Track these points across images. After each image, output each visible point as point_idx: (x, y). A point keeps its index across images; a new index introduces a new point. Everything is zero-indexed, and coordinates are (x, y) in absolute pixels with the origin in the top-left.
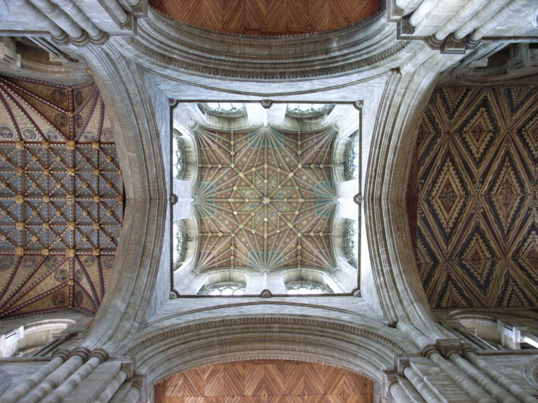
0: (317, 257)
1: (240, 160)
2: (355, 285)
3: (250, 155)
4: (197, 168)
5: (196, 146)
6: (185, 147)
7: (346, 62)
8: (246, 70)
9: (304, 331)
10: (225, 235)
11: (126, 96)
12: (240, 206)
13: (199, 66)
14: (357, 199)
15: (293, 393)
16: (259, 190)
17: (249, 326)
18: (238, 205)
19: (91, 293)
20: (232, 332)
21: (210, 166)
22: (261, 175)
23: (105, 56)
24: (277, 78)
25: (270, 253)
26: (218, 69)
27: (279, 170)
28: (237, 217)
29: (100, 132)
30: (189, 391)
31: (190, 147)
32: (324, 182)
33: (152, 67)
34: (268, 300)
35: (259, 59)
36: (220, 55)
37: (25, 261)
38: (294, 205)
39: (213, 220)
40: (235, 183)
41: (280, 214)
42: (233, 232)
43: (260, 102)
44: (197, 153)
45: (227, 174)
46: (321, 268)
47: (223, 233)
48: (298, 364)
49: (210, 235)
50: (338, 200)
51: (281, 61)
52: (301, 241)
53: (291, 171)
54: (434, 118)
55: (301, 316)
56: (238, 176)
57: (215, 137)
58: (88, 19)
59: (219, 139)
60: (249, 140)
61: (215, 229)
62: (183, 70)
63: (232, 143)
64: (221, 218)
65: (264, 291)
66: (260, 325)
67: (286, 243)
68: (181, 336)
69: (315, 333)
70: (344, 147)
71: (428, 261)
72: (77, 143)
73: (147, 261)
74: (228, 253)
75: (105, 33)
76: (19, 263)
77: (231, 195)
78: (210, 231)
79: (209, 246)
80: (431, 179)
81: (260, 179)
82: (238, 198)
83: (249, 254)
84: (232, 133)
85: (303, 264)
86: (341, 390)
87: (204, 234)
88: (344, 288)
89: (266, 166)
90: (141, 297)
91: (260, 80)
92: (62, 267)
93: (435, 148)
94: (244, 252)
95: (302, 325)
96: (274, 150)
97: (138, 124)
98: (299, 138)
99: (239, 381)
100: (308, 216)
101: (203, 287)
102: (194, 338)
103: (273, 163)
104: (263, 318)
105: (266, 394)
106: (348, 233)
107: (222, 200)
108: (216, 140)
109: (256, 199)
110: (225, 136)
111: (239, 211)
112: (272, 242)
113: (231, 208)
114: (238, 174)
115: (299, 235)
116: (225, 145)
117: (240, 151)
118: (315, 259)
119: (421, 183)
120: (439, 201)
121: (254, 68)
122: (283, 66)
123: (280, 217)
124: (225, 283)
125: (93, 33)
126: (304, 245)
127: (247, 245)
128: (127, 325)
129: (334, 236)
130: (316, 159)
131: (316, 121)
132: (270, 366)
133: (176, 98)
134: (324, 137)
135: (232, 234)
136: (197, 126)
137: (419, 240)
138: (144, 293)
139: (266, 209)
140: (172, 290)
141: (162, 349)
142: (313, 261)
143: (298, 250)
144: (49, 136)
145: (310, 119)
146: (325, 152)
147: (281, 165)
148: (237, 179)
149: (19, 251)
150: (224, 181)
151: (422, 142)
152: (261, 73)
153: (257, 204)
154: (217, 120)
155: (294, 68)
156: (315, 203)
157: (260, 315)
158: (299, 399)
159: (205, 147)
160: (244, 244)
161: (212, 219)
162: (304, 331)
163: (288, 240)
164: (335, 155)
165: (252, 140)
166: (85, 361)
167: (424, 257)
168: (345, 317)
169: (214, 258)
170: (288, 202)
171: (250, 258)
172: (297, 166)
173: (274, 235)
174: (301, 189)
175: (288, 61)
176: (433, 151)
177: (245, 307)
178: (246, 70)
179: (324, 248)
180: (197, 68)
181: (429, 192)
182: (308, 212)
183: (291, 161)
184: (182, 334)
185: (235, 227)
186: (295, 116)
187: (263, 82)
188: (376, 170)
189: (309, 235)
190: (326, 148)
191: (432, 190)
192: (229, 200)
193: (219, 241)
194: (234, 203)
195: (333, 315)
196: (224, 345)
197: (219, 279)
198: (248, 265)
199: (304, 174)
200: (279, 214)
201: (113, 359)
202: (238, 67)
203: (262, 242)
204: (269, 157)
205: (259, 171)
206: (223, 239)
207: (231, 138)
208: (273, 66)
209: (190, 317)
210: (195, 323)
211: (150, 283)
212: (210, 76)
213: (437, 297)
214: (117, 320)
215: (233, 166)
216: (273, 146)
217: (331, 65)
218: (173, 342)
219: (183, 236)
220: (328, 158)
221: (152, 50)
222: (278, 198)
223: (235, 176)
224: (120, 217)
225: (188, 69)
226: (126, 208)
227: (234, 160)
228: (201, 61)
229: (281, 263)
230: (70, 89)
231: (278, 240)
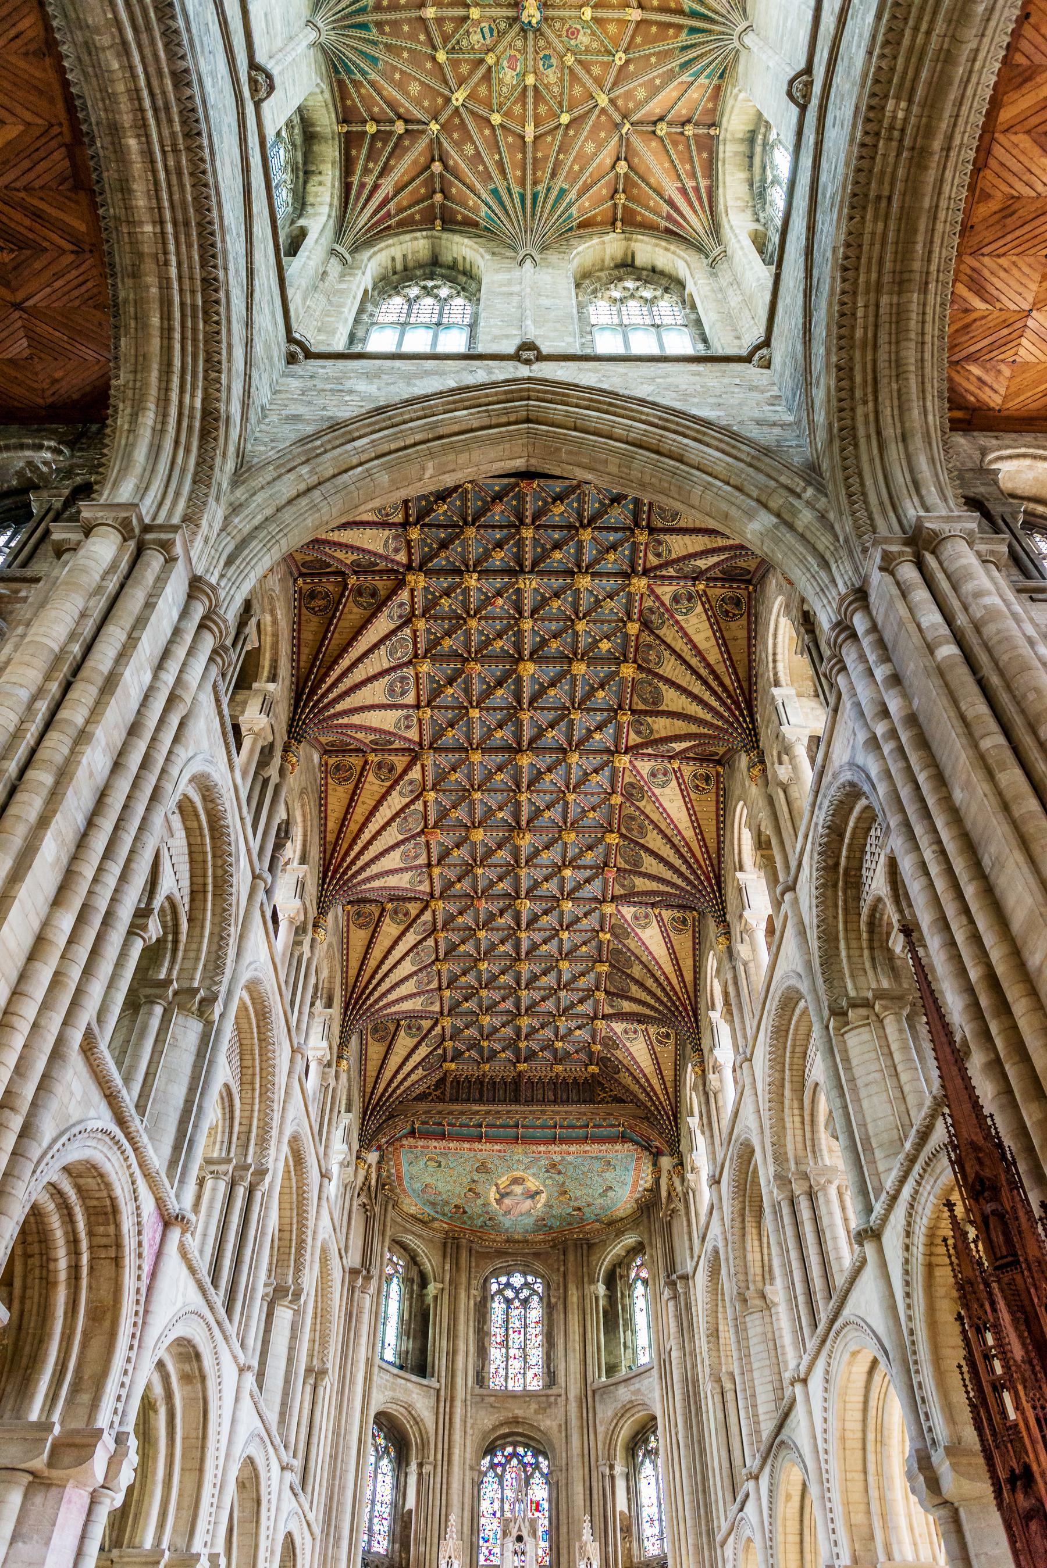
1: (418, 102)
3: (402, 72)
4: (445, 235)
6: (395, 273)
8: (189, 197)
9: (927, 18)
10: (626, 153)
11: (304, 502)
12: (546, 103)
13: (205, 333)
16: (502, 34)
17: (872, 194)
20: (877, 246)
21: (438, 197)
22: (456, 30)
23: (234, 567)
24: (191, 98)
26: (204, 280)
29: (384, 525)
31: (393, 259)
33: (232, 449)
34: (817, 89)
35: (153, 162)
36: (168, 279)
37: (648, 661)
40: (482, 117)
42: (617, 126)
43: (257, 105)
44: (408, 237)
45: (458, 145)
47: (618, 159)
48: (1027, 16)
49: (621, 199)
51: (145, 93)
57: (362, 185)
58: (177, 632)
59: (366, 171)
60: (358, 77)
62: (224, 377)
63: (371, 128)
65: (790, 94)
66: (878, 159)
68: (858, 394)
72: (409, 567)
73: (673, 441)
74: (675, 144)
75: (191, 585)
76: (649, 671)
77: (514, 133)
78: (612, 198)
81: (468, 32)
82: (525, 109)
83: (686, 77)
84: (345, 129)
90: (750, 470)
92: (667, 599)
94: (681, 95)
95: (906, 19)
97: (361, 464)
102: (869, 358)
104: (863, 145)
107: (529, 161)
108: (370, 181)
109: (525, 46)
110: (354, 152)
111: (561, 106)
121: (180, 174)
122: (155, 83)
125: (199, 610)
127: (658, 82)
128: (806, 517)
132: (1006, 115)
133: (284, 346)
144: (400, 617)
148: (472, 113)
149: (628, 671)
150: (478, 153)
152: (188, 149)
154: (315, 179)
155: (153, 43)
157: (849, 153)
159: (388, 215)
160: (654, 91)
161: (580, 195)
162: (927, 18)
165: (357, 66)
166: (854, 636)
169: (683, 191)
175: (140, 69)
177: (823, 178)
178: (189, 197)
180: (213, 338)
184: (852, 390)
193: (642, 170)
196: (906, 276)
198: (715, 81)
201: (865, 580)
202: (187, 224)
203: (654, 29)
205: (446, 39)
208: (163, 115)
209: (819, 349)
212: (223, 301)
214: (789, 537)
215: (435, 127)
218: (866, 416)
221: (198, 464)
223: (462, 120)
224: (567, 483)
225: (219, 362)
228: (195, 330)
230: (300, 581)
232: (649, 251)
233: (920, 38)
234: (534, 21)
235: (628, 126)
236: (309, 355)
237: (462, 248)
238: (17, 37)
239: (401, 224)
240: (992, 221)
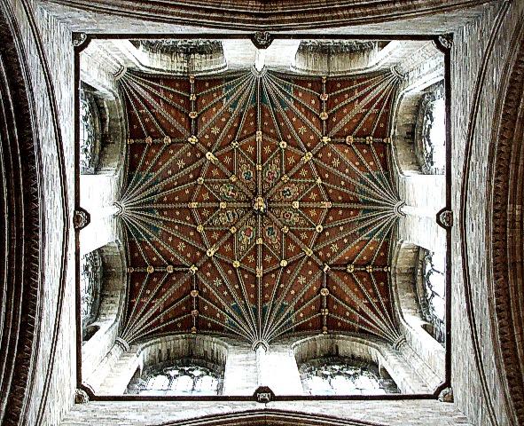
0: (369, 106)
1: (183, 254)
2: (430, 45)
4: (198, 337)
6: (160, 361)
18: (268, 258)
25: (361, 197)
28: (291, 260)
31: (160, 351)
34: (456, 215)
38: (267, 150)
41: (285, 178)
42: (321, 268)
43: (77, 231)
44: (171, 337)
45: (210, 280)
46: (391, 97)
52: (336, 136)
53: (203, 155)
57: (141, 304)
59: (144, 295)
63: (151, 270)
65: (438, 221)
70: (157, 56)
74: (360, 278)
77: (249, 273)
79: (348, 314)
83: (363, 237)
88: (433, 63)
89: (194, 205)
95: (509, 160)
98: (141, 141)
101: (425, 327)
108: (146, 301)
109: (257, 223)
111: (280, 255)
112: (341, 193)
113: (274, 271)
114: (210, 258)
115: (326, 139)
117: (167, 256)
118: (373, 110)
123: (292, 177)
124: (419, 284)
127: (346, 241)
130: (179, 107)
133: (74, 390)
135: (325, 270)
136: (120, 340)
140: (435, 396)
145: (103, 121)
148: (220, 261)
150: (224, 284)
157: (487, 239)
159: (158, 323)
161: (296, 310)
163: (336, 162)
165: (144, 232)
168: (495, 77)
169: (369, 305)
170: (262, 163)
171: (371, 235)
177: (471, 264)
179: (351, 93)
183: (183, 157)
187: (44, 234)
188: (207, 11)
190: (157, 89)
194: (265, 265)
195: (489, 97)
199: (209, 132)
204: (177, 199)
205: (203, 219)
206: (335, 288)
209: (491, 371)
210: (503, 366)
215: (194, 269)
219: (328, 364)
223: (213, 265)
225: (26, 379)
227: (184, 266)
231: (335, 179)
232: (348, 345)
234: (262, 209)
235: (327, 267)
236: (93, 398)
237: (212, 344)
239: (166, 329)
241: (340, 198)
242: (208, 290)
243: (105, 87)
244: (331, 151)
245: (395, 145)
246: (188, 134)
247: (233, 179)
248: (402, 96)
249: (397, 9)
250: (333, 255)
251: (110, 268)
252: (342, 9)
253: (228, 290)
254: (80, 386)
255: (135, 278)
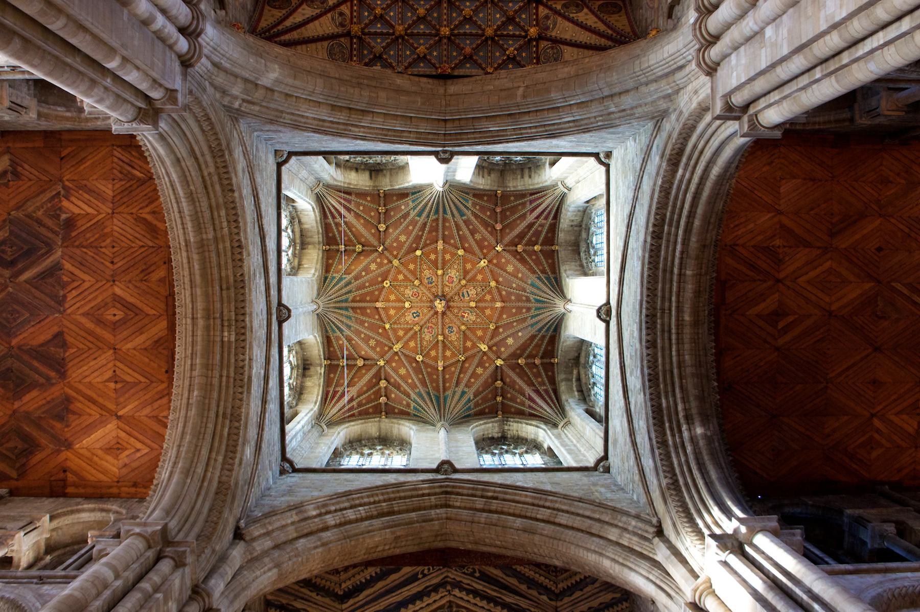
2: (300, 463)
4: (495, 188)
5: (531, 187)
6: (530, 168)
7: (672, 450)
8: (660, 285)
9: (224, 383)
10: (381, 237)
13: (667, 209)
14: (446, 466)
15: (118, 364)
17: (232, 290)
19: (288, 23)
20: (222, 263)
21: (498, 210)
24: (648, 335)
25: (350, 313)
26: (661, 238)
27: (492, 327)
30: (123, 188)
31: (530, 177)
32: (472, 404)
34: (274, 317)
35: (678, 307)
36: (683, 244)
38: (433, 353)
39: (407, 215)
42: (385, 249)
46: (326, 399)
48: (167, 372)
50: (443, 429)
51: (674, 341)
52: (372, 366)
53: (490, 348)
54: (581, 590)
55: (250, 378)
56: (482, 257)
57: (546, 218)
59: (542, 226)
61: (391, 217)
62: (659, 182)
64: (411, 228)
65: (289, 311)
66: (233, 309)
67: (367, 339)
68: (215, 178)
69: (222, 403)
70: (531, 436)
71: (343, 586)
73: (341, 117)
77: (450, 244)
78: (387, 210)
79: (361, 208)
80: (480, 587)
81: (477, 294)
82: (443, 257)
83: (348, 277)
84: (553, 248)
85: (331, 369)
86: (125, 444)
87: (382, 199)
88: (294, 443)
89: (498, 305)
90: (281, 108)
91: (644, 306)
93: (530, 591)
96: (525, 320)
97: (570, 105)
98: (545, 361)
99: (139, 271)
100: (414, 378)
101: (293, 201)
102: (213, 200)
103: (504, 316)
104: (244, 314)
105: (117, 318)
106: (385, 445)
111: (421, 260)
115: (382, 363)
116: (533, 235)
119: (474, 571)
120: (443, 601)
121: (663, 297)
122: (667, 345)
123: (411, 329)
126: (364, 371)
127: (364, 273)
128: (237, 90)
129: (379, 421)
130: (511, 391)
131: (575, 389)
132: (164, 324)
134: (548, 404)
136: (566, 191)
137: (378, 570)
138: (288, 113)
139: (426, 304)
140: (291, 154)
141: (196, 149)
142: (336, 386)
143: (356, 359)
145: (579, 379)
146: (523, 404)
147: (501, 330)
151: (541, 572)
152: (655, 309)
153: (433, 290)
155: (664, 364)
156: (437, 389)
158: (110, 374)
159: (531, 202)
160: (366, 269)
162: (224, 383)
163: (372, 343)
164: (518, 422)
166: (182, 30)
167: (349, 579)
168: (249, 452)
171: (341, 279)
172: (498, 357)
173: (381, 319)
174: (460, 365)
175: (674, 353)
176: (526, 590)
177: (262, 281)
178: (660, 285)
179: (360, 405)
180: (662, 205)
181: (458, 585)
182: (420, 376)
184: (220, 179)
185: (395, 253)
186: (583, 354)
187: (641, 312)
189: (381, 379)
191: (462, 589)
192: (440, 242)
194: (435, 251)
195: (252, 432)
196: (201, 250)
197: (306, 226)
199: (485, 368)
200: (417, 328)
201: (185, 75)
202: (665, 271)
203: (368, 298)
206: (373, 231)
207: (546, 245)
208: (666, 329)
209: (246, 191)
210: (237, 200)
211: (305, 123)
212: (650, 225)
213: (284, 602)
214: (246, 75)
215: (499, 248)
216: (533, 317)
217: (667, 425)
218: (207, 166)
220: (513, 410)
222: (443, 325)
223: (482, 251)
224: (415, 70)
225: (660, 192)
226: (430, 81)
227: (508, 251)
228: (673, 213)
229: (334, 331)
232: (359, 180)
233: (225, 373)
237: (484, 183)
238: (736, 357)
240: (153, 268)
241: (368, 311)
242: (487, 230)
243: (576, 413)
244: (377, 353)
245: (320, 359)
246: (504, 368)
247: (463, 328)
248: (316, 403)
249: (333, 504)
250: (374, 261)
251: (573, 250)
252: (379, 502)
253: (469, 229)
254: (607, 166)
255: (551, 239)
